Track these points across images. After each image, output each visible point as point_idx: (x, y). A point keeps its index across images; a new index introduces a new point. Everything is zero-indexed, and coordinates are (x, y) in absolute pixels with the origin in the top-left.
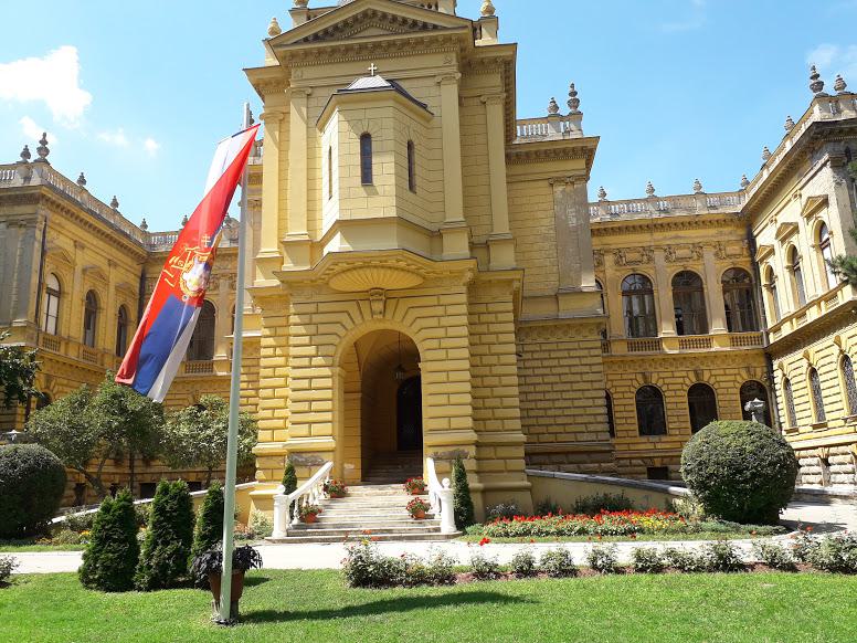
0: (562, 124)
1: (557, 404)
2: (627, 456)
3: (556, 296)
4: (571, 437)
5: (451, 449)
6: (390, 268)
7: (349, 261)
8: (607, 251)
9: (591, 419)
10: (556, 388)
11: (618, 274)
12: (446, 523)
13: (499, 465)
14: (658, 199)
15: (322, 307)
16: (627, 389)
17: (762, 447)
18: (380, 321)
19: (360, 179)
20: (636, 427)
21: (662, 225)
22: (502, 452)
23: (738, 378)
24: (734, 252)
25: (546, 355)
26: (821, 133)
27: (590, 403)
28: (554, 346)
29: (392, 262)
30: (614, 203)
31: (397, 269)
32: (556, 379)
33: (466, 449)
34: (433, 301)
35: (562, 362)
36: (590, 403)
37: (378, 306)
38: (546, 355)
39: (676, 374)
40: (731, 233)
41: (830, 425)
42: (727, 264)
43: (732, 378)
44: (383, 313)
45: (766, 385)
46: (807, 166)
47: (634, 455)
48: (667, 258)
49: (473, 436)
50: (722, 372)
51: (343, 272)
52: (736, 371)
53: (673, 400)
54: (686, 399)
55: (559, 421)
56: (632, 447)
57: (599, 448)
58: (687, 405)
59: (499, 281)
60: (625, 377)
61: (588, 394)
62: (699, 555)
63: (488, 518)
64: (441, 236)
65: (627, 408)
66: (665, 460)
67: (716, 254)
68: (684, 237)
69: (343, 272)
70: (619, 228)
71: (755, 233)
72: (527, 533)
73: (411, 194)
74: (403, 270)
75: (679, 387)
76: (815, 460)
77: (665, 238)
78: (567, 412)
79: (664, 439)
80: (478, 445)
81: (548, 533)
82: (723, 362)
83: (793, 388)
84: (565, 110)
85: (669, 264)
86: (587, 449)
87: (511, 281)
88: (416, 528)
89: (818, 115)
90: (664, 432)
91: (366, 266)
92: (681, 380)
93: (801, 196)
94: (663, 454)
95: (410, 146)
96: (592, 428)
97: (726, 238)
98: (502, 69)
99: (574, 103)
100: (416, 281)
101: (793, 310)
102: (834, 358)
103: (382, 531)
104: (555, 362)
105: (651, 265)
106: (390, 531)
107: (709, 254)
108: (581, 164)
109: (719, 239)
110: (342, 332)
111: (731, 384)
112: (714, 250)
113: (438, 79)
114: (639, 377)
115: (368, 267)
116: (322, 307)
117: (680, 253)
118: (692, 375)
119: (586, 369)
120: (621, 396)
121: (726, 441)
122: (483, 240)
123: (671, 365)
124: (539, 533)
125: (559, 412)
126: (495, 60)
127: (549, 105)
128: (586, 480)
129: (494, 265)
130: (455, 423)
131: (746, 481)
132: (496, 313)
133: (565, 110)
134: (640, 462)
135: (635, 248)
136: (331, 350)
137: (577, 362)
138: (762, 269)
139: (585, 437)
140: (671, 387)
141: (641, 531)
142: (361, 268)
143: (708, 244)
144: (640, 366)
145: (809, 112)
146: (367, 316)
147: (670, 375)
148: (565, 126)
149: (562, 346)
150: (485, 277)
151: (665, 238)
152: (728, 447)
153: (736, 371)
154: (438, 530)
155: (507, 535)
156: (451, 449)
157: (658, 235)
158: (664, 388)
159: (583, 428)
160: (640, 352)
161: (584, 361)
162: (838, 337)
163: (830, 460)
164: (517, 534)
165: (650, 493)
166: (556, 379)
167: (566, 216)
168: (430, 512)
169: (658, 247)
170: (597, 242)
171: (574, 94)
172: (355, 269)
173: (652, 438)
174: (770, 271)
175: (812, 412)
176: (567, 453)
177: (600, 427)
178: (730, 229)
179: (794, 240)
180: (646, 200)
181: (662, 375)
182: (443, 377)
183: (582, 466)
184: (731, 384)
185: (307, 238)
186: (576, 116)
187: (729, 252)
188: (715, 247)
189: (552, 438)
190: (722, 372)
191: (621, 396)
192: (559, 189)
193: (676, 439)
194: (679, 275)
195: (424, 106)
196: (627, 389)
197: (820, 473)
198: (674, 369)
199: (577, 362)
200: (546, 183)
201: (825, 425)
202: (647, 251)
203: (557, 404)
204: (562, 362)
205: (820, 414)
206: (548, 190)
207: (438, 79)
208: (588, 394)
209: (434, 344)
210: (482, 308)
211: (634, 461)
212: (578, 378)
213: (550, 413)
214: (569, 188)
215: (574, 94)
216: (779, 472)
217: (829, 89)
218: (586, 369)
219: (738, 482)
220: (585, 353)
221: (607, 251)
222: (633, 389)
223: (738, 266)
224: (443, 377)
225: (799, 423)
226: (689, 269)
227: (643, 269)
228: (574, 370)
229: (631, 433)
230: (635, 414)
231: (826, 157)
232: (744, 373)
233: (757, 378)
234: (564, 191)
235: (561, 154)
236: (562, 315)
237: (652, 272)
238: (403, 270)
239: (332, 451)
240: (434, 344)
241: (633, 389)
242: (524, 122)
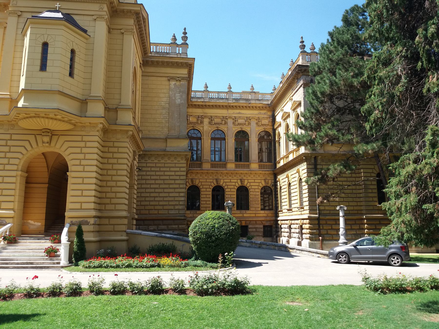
0: (177, 48)
1: (161, 195)
3: (166, 139)
4: (166, 212)
5: (79, 220)
6: (52, 118)
7: (27, 113)
8: (206, 117)
9: (177, 203)
10: (161, 186)
11: (210, 129)
12: (64, 261)
13: (111, 228)
14: (233, 93)
15: (14, 137)
16: (208, 187)
17: (223, 225)
18: (47, 147)
19: (39, 68)
20: (211, 206)
21: (233, 106)
22: (113, 221)
23: (260, 184)
24: (265, 123)
25: (158, 169)
26: (301, 70)
27: (177, 195)
28: (163, 165)
29: (52, 116)
30: (211, 92)
31: (56, 119)
32: (162, 182)
33: (89, 220)
34: (79, 138)
35: (166, 173)
36: (177, 195)
37: (46, 139)
38: (158, 169)
39: (232, 181)
40: (265, 114)
41: (293, 210)
42: (261, 129)
43: (258, 184)
44: (50, 143)
45: (273, 188)
46: (295, 86)
48: (233, 123)
49: (93, 213)
50: (253, 181)
51: (24, 118)
52: (260, 181)
53: (229, 193)
54: (235, 193)
55: (161, 203)
57: (178, 218)
58: (235, 196)
59: (121, 130)
60: (208, 180)
61: (177, 190)
62: (143, 285)
63: (97, 256)
64: (87, 103)
65: (207, 196)
67: (257, 124)
68: (243, 114)
69: (24, 118)
70: (212, 105)
71: (276, 115)
72: (100, 266)
73: (70, 79)
74: (60, 120)
75: (233, 187)
76: (286, 226)
77: (233, 113)
78: (165, 199)
80: (95, 217)
81: (111, 267)
82: (254, 176)
83: (292, 188)
84: (179, 41)
85: (234, 126)
86: (173, 218)
87: (127, 131)
88: (47, 262)
89: (300, 62)
91: (37, 116)
92: (234, 184)
93: (292, 99)
95: (73, 52)
96: (177, 207)
97: (263, 116)
98: (134, 17)
99: (185, 38)
100: (67, 126)
101: (285, 154)
102: (296, 179)
103: (27, 263)
104: (162, 173)
105: (226, 126)
106: (32, 263)
107: (253, 123)
108: (184, 72)
109: (259, 116)
110: (24, 152)
111: (257, 187)
112: (256, 121)
113: (94, 17)
114: (215, 181)
115: (39, 117)
116: (14, 137)
117: (240, 121)
118: (239, 181)
119: (178, 178)
121: (207, 222)
122: (115, 107)
123: (230, 176)
124: (107, 267)
125: (162, 199)
126: (130, 11)
127: (172, 37)
128: (156, 236)
129: (118, 121)
130: (85, 206)
131: (213, 242)
132: (118, 147)
133: (179, 41)
135: (219, 117)
136: (16, 161)
137: (173, 173)
138: (277, 132)
139: (171, 212)
140: (229, 187)
141: (159, 266)
142: (35, 117)
143: (253, 118)
144: (215, 176)
145: (298, 59)
146: (40, 144)
147: (229, 181)
148: (179, 50)
149: (166, 165)
150: (114, 127)
151: (233, 113)
152: (208, 225)
153: (260, 181)
154: (59, 263)
155: (90, 267)
156: (79, 220)
157: (231, 111)
158: (226, 187)
159: (172, 207)
160: (215, 169)
161: (177, 174)
162: (298, 169)
163: (292, 226)
164: (95, 267)
165: (185, 243)
166: (162, 182)
167: (175, 98)
168: (58, 253)
169: (230, 117)
170: (199, 112)
171: (185, 33)
172: (31, 117)
174: (279, 133)
175: (298, 201)
176: (163, 220)
177: (180, 207)
178: (265, 111)
179: (288, 120)
180: (226, 93)
181: (225, 181)
182: (80, 181)
183: (169, 226)
184: (257, 187)
185: (8, 97)
186: (185, 45)
187: (263, 123)
188: (257, 120)
189: (156, 212)
190: (253, 181)
192: (173, 83)
194: (239, 132)
195: (85, 31)
196: (208, 187)
197: (288, 232)
198: (231, 178)
199: (173, 173)
200: (167, 78)
201: (291, 210)
202: (225, 119)
203: (161, 195)
204: (166, 173)
205: (290, 205)
206: (167, 83)
207: (94, 17)
208: (177, 190)
209: (77, 162)
210: (111, 144)
212: (173, 182)
213: (156, 199)
214: (178, 83)
215: (185, 33)
216: (228, 238)
217: (308, 50)
218: (178, 178)
219: (210, 242)
220: (178, 169)
221: (206, 117)
222: (211, 187)
223: (266, 130)
224: (80, 181)
225: (293, 206)
226: (243, 129)
227: (222, 127)
228: (171, 177)
230: (211, 199)
231: (301, 82)
232: (263, 182)
233: (269, 185)
234: (175, 84)
235: (175, 65)
236: (168, 149)
237: (226, 129)
238: (60, 120)
239: (12, 218)
240: (77, 162)
241: (211, 187)
242: (157, 44)
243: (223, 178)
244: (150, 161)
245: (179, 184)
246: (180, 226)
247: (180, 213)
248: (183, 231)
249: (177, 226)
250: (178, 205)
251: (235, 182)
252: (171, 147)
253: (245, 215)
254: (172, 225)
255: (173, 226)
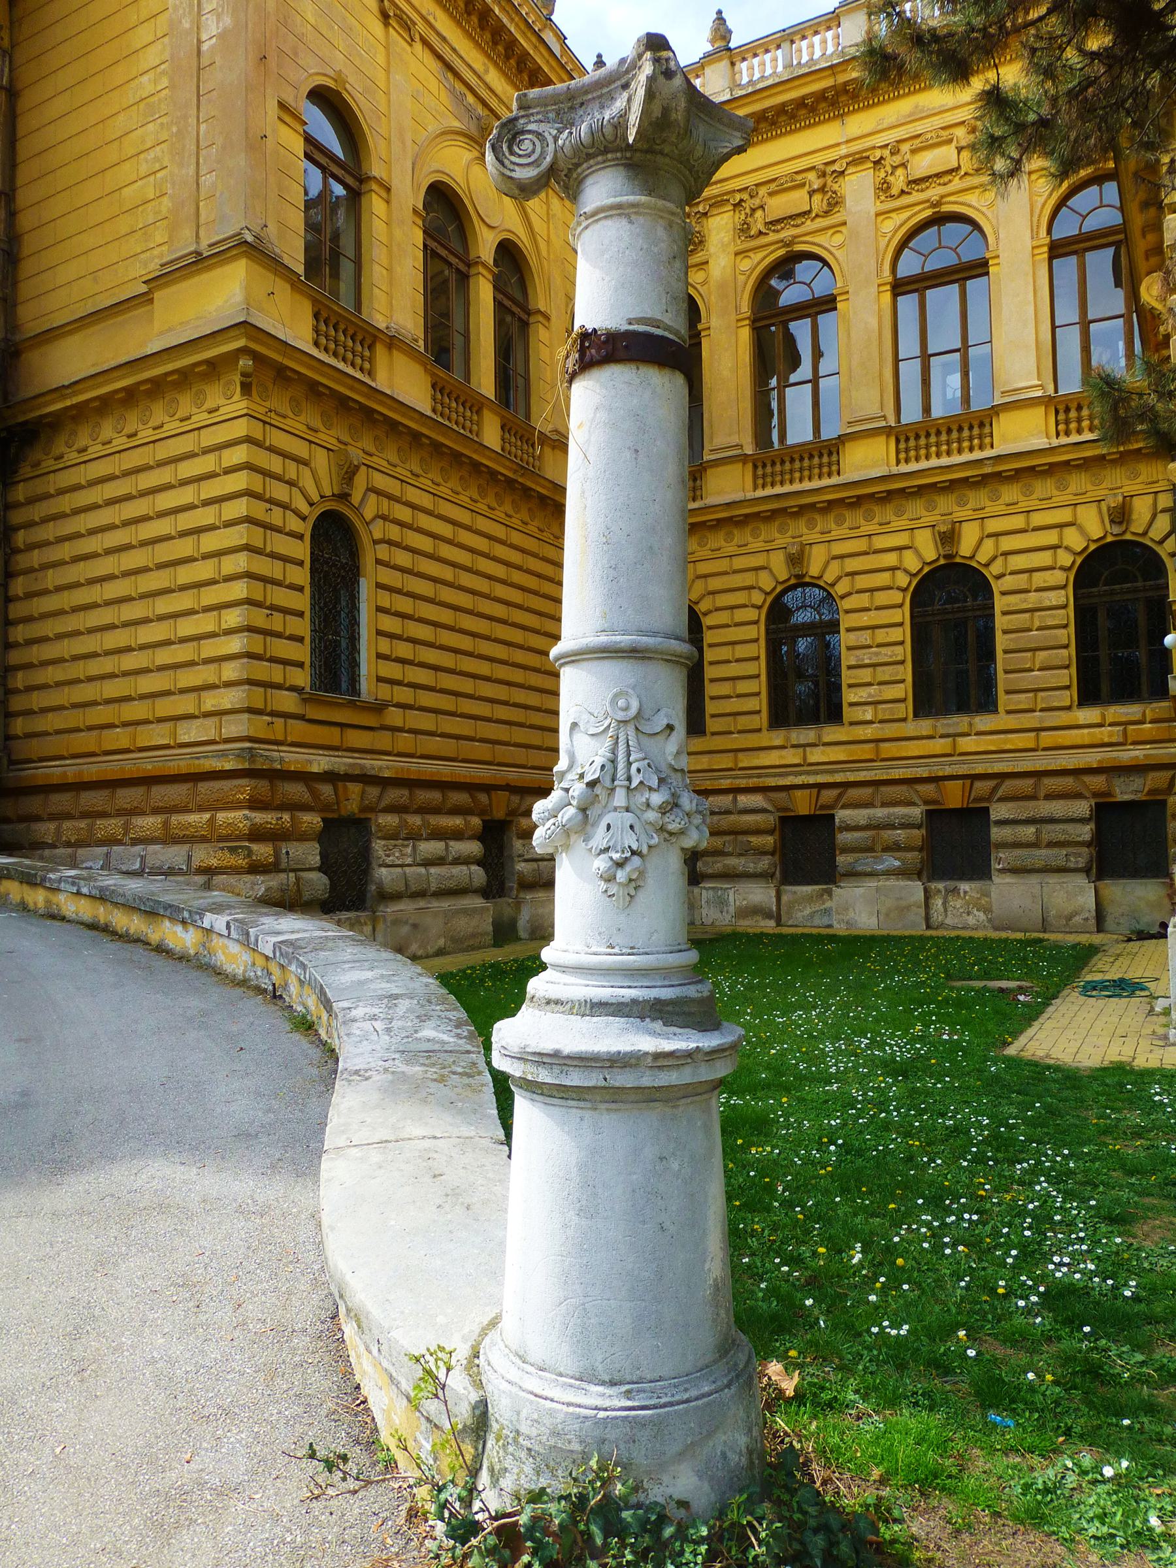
2: (725, 784)
20: (761, 703)
36: (206, 624)
43: (1051, 538)
47: (743, 783)
50: (1018, 522)
56: (745, 761)
66: (828, 795)
79: (832, 733)
86: (182, 766)
90: (835, 715)
92: (891, 559)
94: (820, 779)
120: (722, 618)
134: (756, 800)
139: (190, 732)
140: (863, 582)
147: (860, 545)
153: (1065, 515)
173: (807, 734)
183: (175, 819)
184: (1045, 558)
191: (722, 618)
193: (868, 732)
211: (744, 800)
229: (744, 722)
243: (827, 537)
244: (95, 450)
245: (219, 554)
246: (221, 816)
247: (226, 733)
248: (232, 850)
249: (207, 816)
250: (214, 687)
251: (900, 549)
252: (170, 330)
253: (967, 744)
254: (190, 811)
255: (193, 818)
